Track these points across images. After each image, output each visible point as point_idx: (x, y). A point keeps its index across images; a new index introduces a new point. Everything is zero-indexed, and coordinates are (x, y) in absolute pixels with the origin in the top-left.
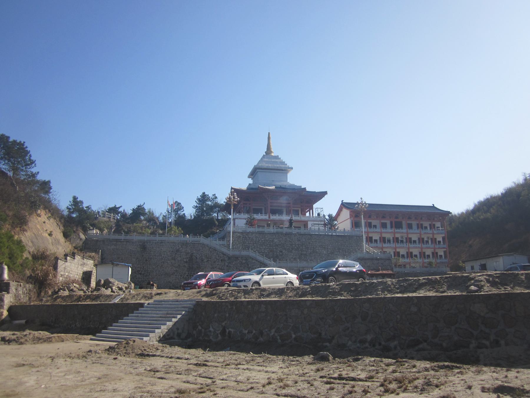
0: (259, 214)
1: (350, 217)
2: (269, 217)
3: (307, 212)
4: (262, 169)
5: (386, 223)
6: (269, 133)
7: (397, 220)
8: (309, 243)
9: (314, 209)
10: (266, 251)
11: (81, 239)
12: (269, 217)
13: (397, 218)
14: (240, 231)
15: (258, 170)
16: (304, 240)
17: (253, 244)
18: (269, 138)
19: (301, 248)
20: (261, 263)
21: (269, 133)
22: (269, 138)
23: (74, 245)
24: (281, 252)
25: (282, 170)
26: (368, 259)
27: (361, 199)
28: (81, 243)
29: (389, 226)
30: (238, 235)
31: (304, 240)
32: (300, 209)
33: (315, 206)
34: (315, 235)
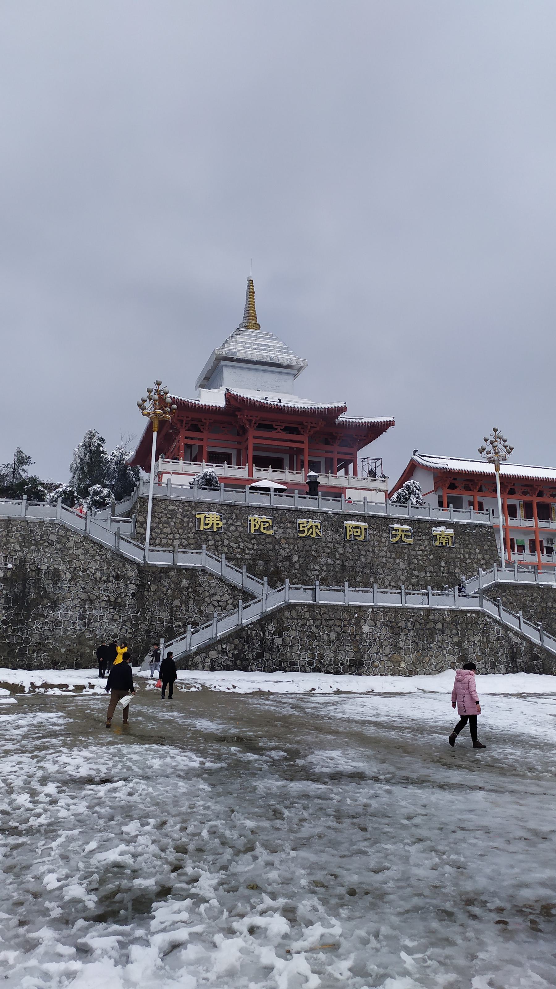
0: (226, 465)
1: (436, 489)
2: (251, 474)
3: (339, 469)
4: (230, 359)
5: (515, 506)
6: (251, 282)
7: (541, 500)
9: (359, 462)
10: (247, 557)
12: (251, 474)
13: (540, 495)
14: (174, 497)
15: (223, 363)
18: (251, 293)
19: (341, 551)
20: (235, 588)
21: (251, 282)
22: (251, 293)
27: (495, 430)
29: (520, 512)
30: (171, 507)
32: (323, 461)
33: (362, 454)
34: (378, 517)
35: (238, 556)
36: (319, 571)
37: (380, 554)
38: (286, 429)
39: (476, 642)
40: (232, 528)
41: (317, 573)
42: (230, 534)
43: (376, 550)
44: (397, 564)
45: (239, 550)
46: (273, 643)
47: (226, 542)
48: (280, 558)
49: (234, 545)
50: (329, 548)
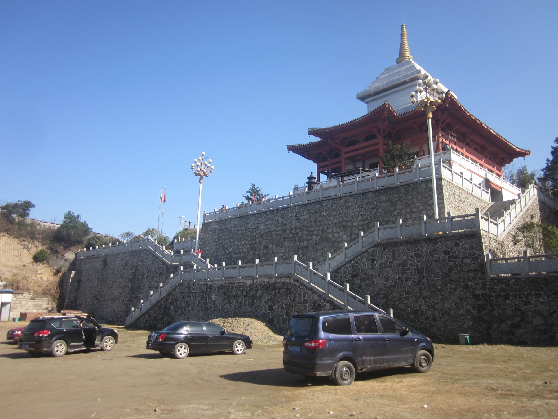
8: (316, 221)
11: (66, 260)
16: (307, 217)
17: (230, 239)
23: (56, 268)
24: (266, 247)
25: (405, 83)
26: (405, 242)
28: (68, 264)
31: (307, 217)
35: (241, 250)
36: (283, 253)
37: (328, 231)
38: (368, 138)
39: (284, 306)
40: (240, 232)
41: (282, 254)
42: (238, 237)
43: (325, 229)
44: (340, 237)
45: (241, 246)
46: (169, 310)
47: (236, 242)
48: (262, 248)
49: (239, 243)
50: (292, 233)
